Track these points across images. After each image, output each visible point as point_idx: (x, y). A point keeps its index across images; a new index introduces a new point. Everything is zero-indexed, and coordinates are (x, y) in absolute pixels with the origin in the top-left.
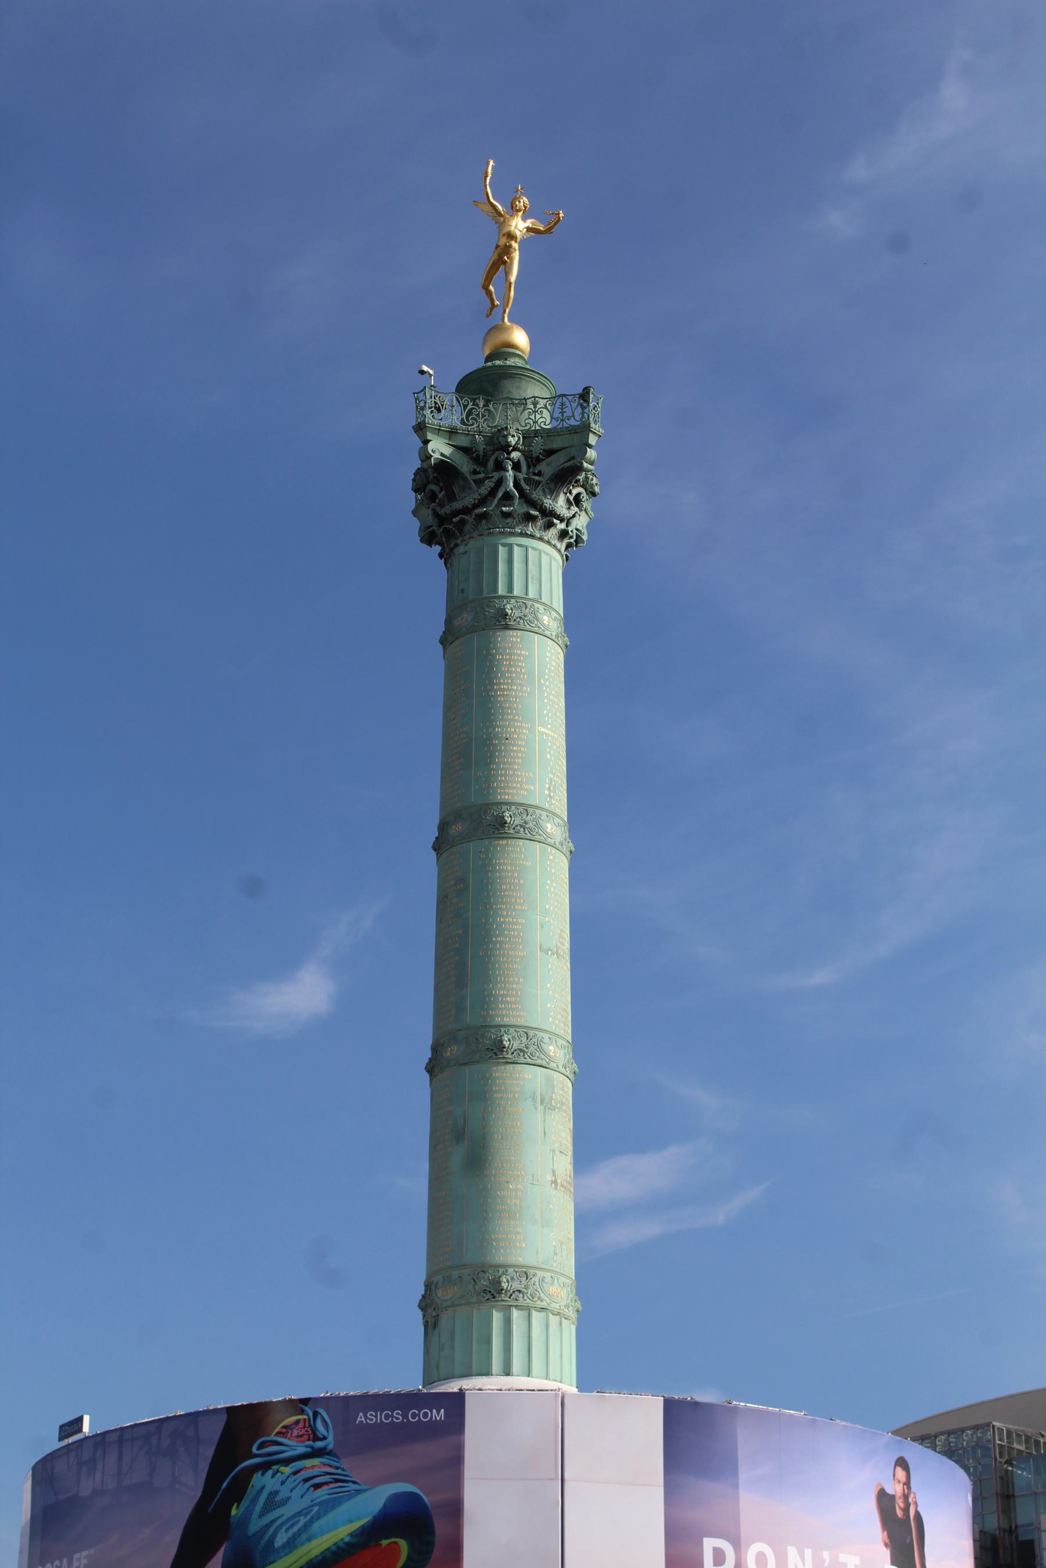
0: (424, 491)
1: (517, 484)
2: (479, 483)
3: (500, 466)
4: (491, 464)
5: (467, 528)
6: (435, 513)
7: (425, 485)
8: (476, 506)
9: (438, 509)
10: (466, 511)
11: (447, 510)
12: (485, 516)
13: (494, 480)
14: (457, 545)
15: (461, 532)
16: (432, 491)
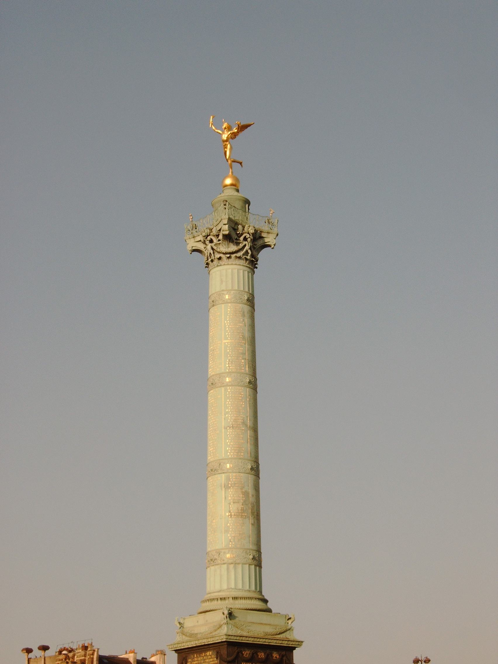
0: (207, 238)
1: (250, 249)
3: (245, 239)
4: (242, 238)
6: (212, 249)
7: (208, 236)
9: (215, 248)
12: (240, 258)
13: (244, 244)
16: (211, 239)
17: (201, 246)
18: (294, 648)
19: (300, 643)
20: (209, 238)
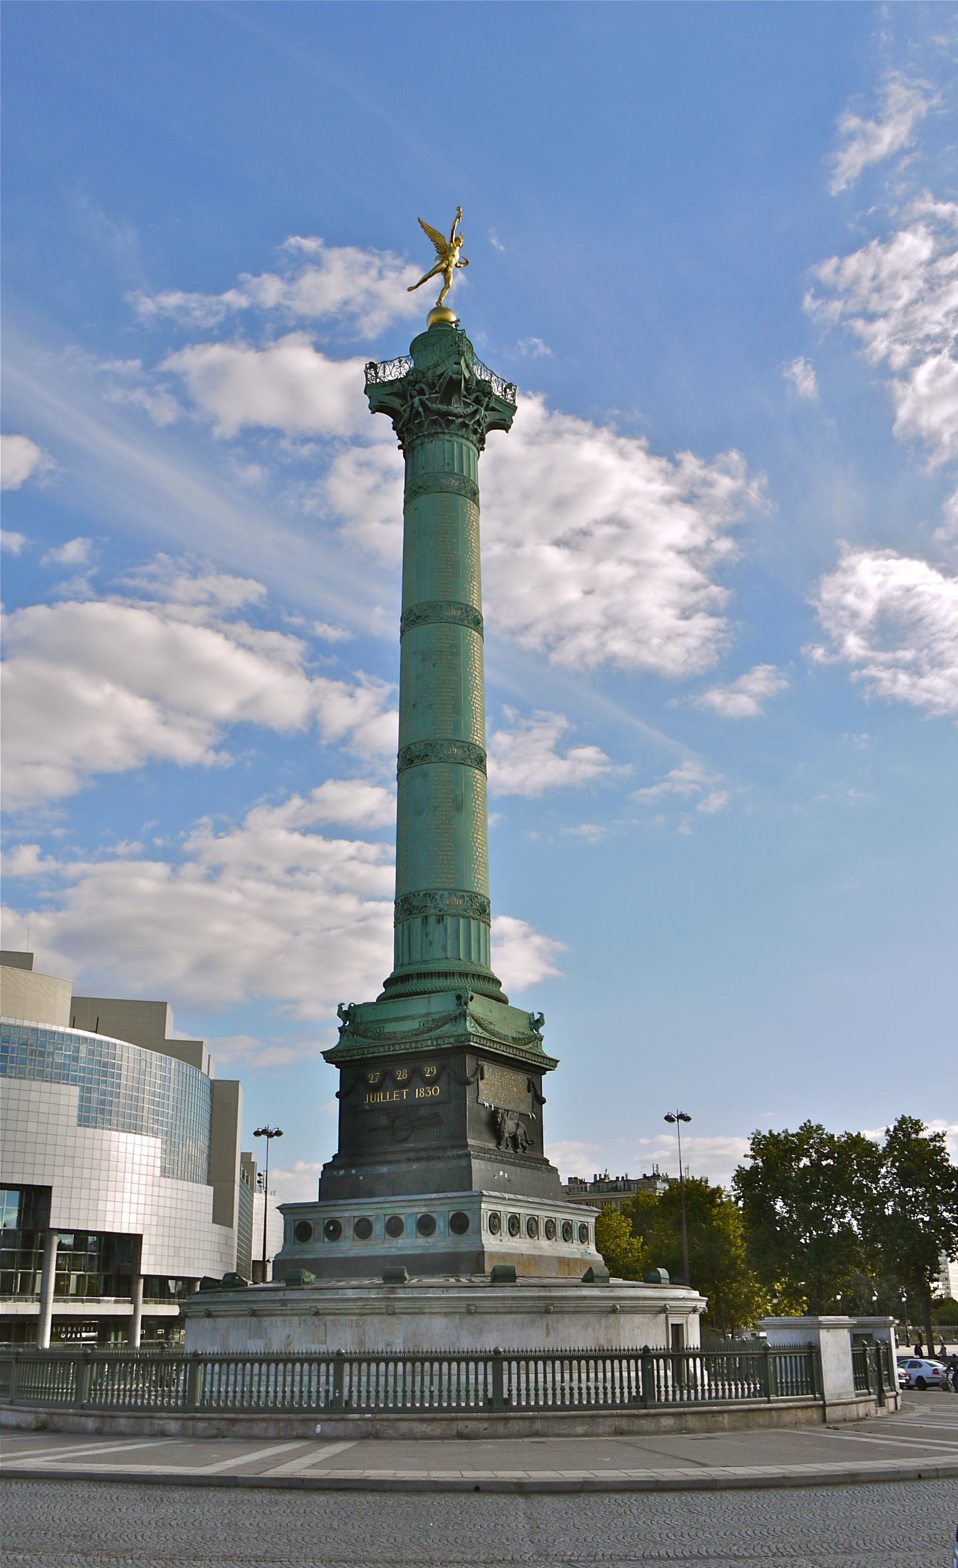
0: (414, 386)
2: (467, 405)
5: (452, 426)
6: (422, 403)
7: (417, 382)
8: (461, 417)
10: (458, 416)
11: (443, 407)
14: (444, 433)
15: (448, 427)
17: (396, 403)
18: (544, 1071)
19: (553, 1063)
20: (417, 387)
